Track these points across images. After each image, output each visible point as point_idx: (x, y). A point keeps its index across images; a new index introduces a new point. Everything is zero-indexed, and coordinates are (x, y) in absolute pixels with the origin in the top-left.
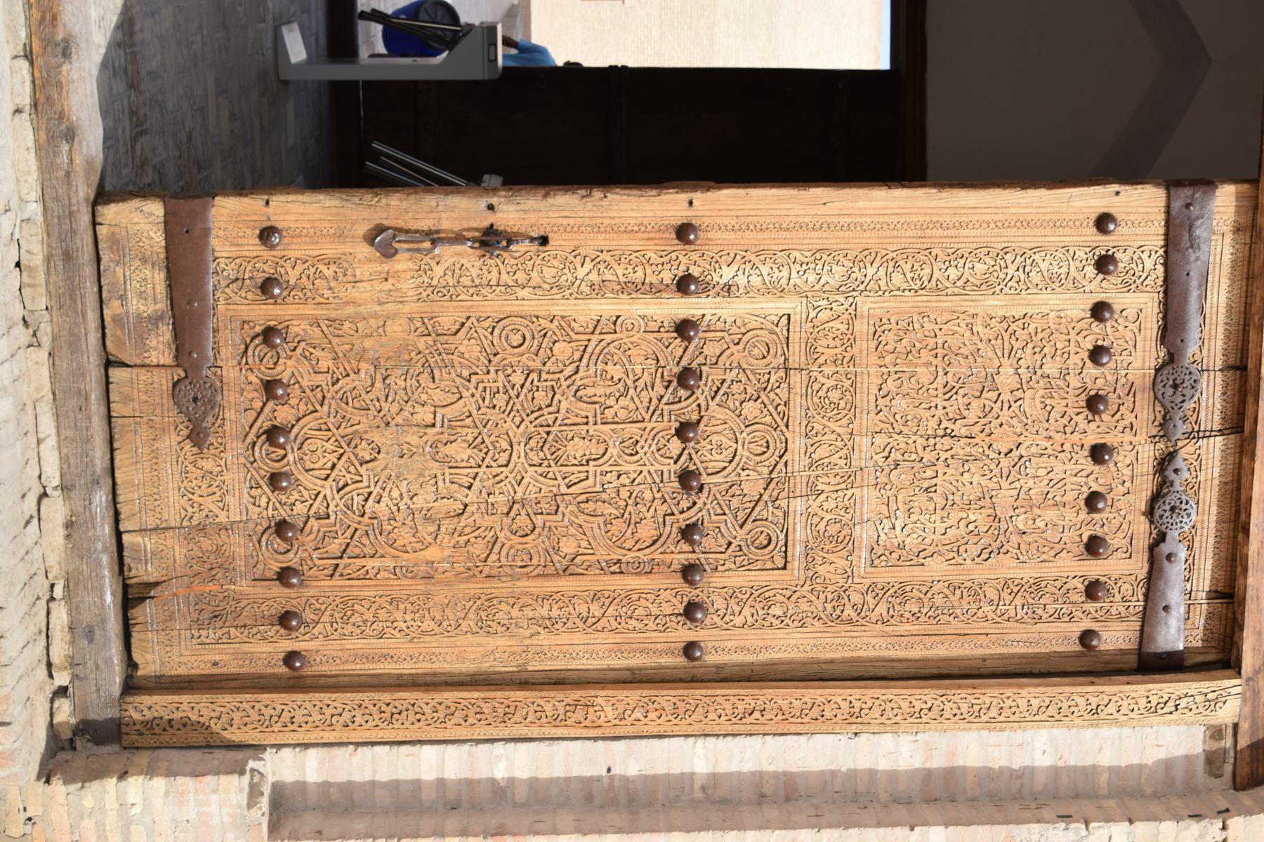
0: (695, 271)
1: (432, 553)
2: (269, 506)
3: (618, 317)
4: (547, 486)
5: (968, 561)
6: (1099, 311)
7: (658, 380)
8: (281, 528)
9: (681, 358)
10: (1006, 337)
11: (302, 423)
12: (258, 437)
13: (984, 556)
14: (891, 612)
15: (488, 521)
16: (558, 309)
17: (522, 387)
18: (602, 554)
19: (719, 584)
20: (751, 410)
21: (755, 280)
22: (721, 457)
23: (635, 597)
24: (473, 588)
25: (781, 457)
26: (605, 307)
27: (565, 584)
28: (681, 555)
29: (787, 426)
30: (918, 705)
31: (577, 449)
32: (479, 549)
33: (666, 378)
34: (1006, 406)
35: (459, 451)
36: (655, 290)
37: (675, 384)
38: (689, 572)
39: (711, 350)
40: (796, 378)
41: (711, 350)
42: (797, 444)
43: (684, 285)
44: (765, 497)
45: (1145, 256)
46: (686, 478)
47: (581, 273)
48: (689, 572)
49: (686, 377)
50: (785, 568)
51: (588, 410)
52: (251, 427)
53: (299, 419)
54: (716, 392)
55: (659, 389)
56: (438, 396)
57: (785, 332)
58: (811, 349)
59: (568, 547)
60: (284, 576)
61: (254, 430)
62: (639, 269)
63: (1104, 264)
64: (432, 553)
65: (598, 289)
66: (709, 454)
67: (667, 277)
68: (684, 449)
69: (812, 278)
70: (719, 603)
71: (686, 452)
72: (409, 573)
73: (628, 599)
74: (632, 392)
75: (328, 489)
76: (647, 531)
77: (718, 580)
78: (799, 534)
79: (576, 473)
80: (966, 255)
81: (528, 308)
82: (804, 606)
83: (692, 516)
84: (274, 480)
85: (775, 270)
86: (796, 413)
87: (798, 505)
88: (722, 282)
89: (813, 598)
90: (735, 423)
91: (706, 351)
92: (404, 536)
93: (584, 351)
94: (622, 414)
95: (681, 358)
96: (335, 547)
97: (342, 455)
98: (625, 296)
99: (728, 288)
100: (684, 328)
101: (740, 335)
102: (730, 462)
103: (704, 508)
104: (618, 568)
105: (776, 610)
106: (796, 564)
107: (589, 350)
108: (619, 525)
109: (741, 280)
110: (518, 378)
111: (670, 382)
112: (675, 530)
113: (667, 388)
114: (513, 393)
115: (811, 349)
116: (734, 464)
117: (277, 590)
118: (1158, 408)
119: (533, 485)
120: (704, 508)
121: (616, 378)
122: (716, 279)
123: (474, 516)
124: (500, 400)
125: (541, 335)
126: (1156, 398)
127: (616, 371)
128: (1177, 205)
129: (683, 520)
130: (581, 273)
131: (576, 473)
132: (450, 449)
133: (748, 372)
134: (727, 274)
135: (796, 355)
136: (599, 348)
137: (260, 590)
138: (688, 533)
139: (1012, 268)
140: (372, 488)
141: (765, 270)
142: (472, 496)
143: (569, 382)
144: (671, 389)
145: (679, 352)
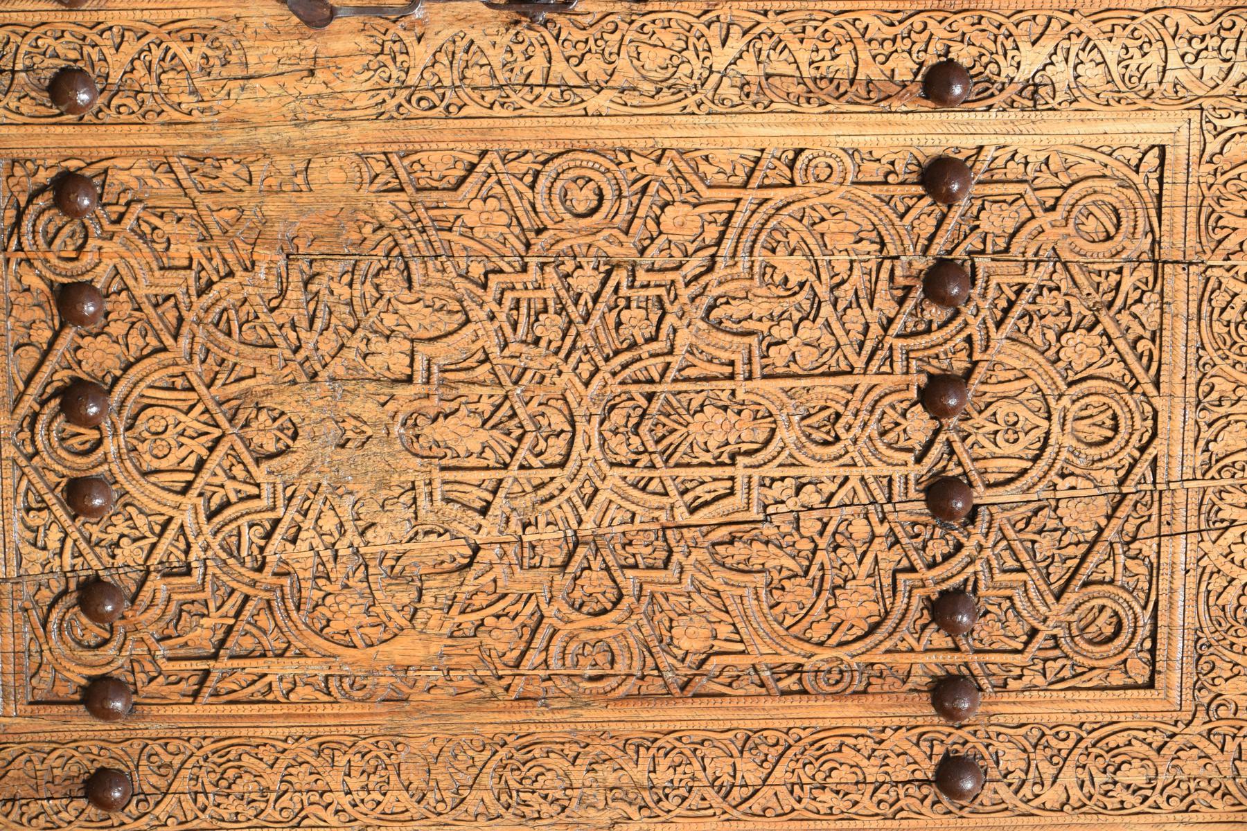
0: (963, 56)
1: (406, 649)
2: (62, 547)
4: (646, 506)
7: (883, 285)
8: (91, 593)
9: (931, 238)
11: (134, 373)
12: (43, 404)
15: (524, 581)
16: (677, 132)
17: (596, 298)
18: (763, 653)
19: (1012, 715)
20: (1080, 349)
21: (1091, 74)
22: (1015, 449)
23: (832, 744)
24: (491, 722)
25: (1142, 450)
26: (772, 132)
27: (681, 714)
28: (930, 655)
29: (1157, 384)
31: (711, 430)
32: (503, 639)
33: (900, 281)
35: (464, 435)
36: (878, 96)
37: (917, 294)
38: (946, 692)
39: (995, 221)
40: (1175, 280)
41: (995, 221)
42: (1176, 423)
43: (938, 83)
44: (1109, 534)
46: (942, 494)
47: (721, 59)
48: (946, 692)
49: (942, 280)
50: (1150, 685)
51: (736, 349)
52: (28, 382)
53: (128, 366)
54: (1006, 311)
55: (885, 303)
56: (420, 319)
57: (1154, 185)
58: (1209, 220)
59: (691, 638)
60: (96, 694)
61: (35, 389)
62: (845, 49)
64: (406, 649)
65: (756, 95)
66: (989, 445)
67: (903, 67)
68: (936, 432)
69: (1212, 67)
70: (1012, 759)
71: (942, 437)
72: (353, 688)
73: (819, 747)
74: (826, 310)
75: (188, 513)
76: (857, 606)
77: (1009, 709)
78: (1181, 615)
79: (709, 480)
81: (609, 132)
82: (1192, 767)
83: (952, 574)
84: (77, 494)
85: (1137, 53)
86: (1175, 356)
87: (1177, 551)
88: (1021, 76)
89: (1211, 750)
90: (1046, 377)
91: (985, 225)
92: (347, 613)
94: (807, 358)
95: (931, 238)
96: (202, 634)
97: (217, 441)
98: (813, 108)
99: (1033, 93)
100: (938, 176)
101: (1057, 190)
102: (1036, 459)
103: (978, 557)
104: (796, 682)
105: (1134, 775)
106: (1173, 678)
107: (738, 220)
108: (799, 592)
109: (1061, 74)
110: (586, 281)
111: (908, 289)
112: (915, 602)
113: (901, 302)
114: (575, 313)
115: (1209, 220)
116: (1043, 464)
117: (82, 724)
119: (618, 505)
120: (978, 557)
121: (793, 282)
122: (1007, 71)
123: (495, 570)
124: (550, 326)
125: (638, 190)
127: (795, 268)
129: (933, 581)
131: (709, 480)
132: (443, 431)
133: (1075, 270)
134: (1031, 59)
135: (1178, 235)
137: (46, 723)
138: (945, 608)
140: (280, 512)
141: (1112, 52)
142: (490, 529)
143: (695, 288)
144: (909, 305)
145: (929, 225)
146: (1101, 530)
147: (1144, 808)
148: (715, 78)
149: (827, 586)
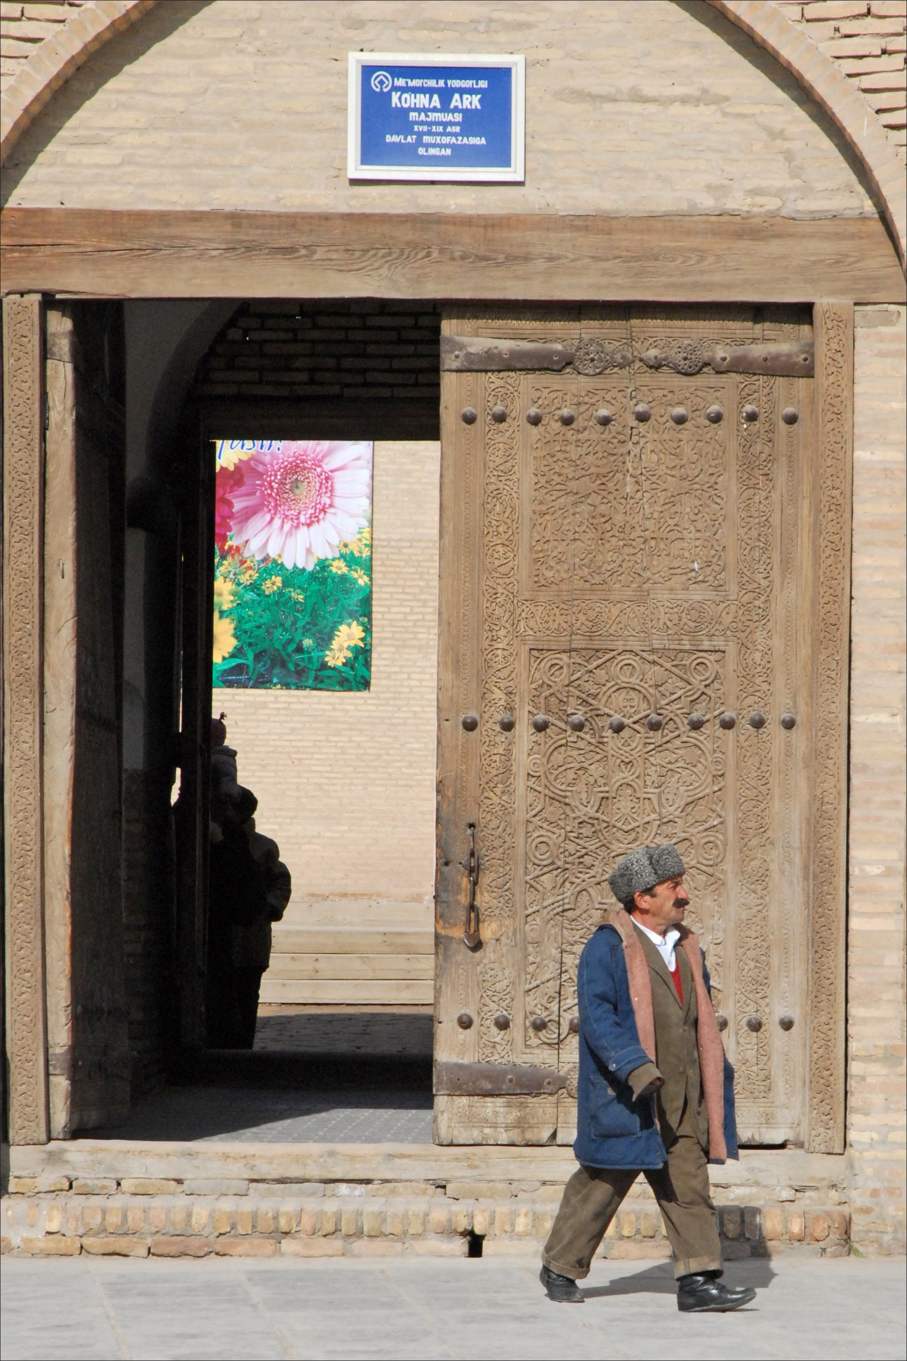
3: (529, 774)
5: (723, 512)
6: (535, 421)
10: (550, 488)
13: (718, 500)
14: (762, 570)
17: (578, 845)
22: (636, 699)
30: (828, 551)
34: (603, 487)
37: (578, 733)
44: (668, 665)
45: (493, 386)
47: (496, 800)
50: (724, 652)
54: (587, 702)
62: (494, 758)
63: (500, 418)
71: (632, 725)
74: (585, 765)
80: (489, 520)
85: (497, 659)
88: (504, 697)
93: (553, 799)
98: (513, 768)
102: (640, 692)
107: (552, 795)
112: (693, 734)
113: (582, 739)
114: (584, 851)
118: (607, 372)
121: (575, 777)
122: (502, 702)
126: (600, 373)
128: (455, 365)
130: (496, 800)
133: (573, 678)
136: (552, 788)
139: (501, 485)
143: (576, 810)
146: (667, 670)
147: (769, 652)
148: (503, 803)
149: (685, 765)
